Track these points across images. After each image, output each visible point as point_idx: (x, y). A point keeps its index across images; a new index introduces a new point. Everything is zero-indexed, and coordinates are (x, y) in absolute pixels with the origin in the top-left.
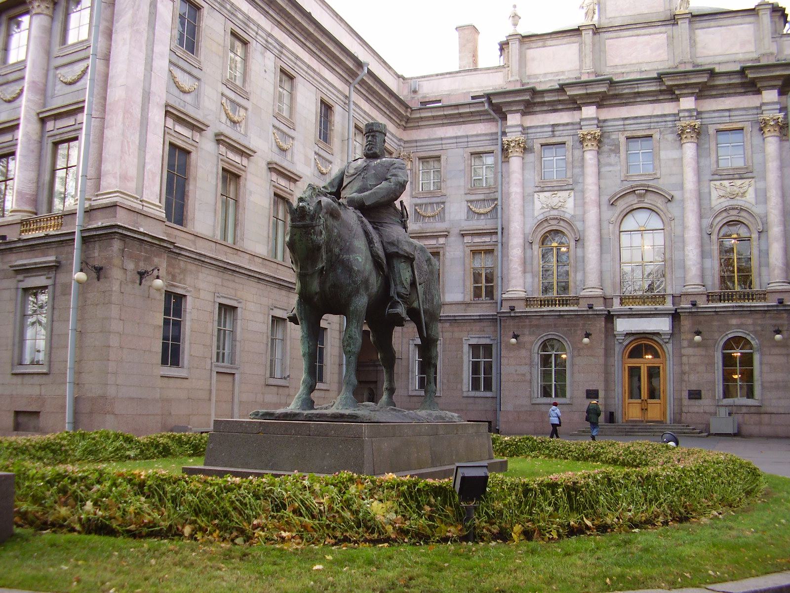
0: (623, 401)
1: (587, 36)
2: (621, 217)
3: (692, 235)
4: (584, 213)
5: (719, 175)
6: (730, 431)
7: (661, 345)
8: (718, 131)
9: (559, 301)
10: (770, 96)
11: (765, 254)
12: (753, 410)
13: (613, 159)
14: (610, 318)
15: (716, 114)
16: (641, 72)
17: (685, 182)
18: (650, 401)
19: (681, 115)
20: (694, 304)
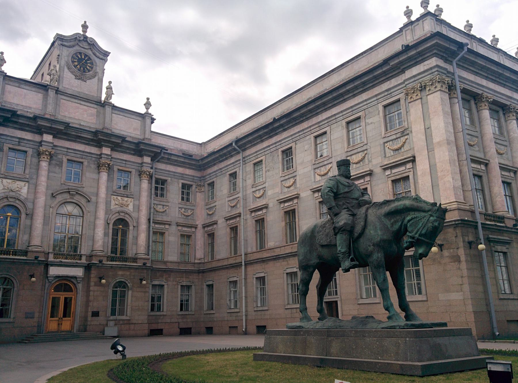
0: (47, 320)
1: (51, 93)
2: (58, 205)
3: (100, 223)
4: (35, 198)
5: (115, 193)
6: (116, 335)
7: (75, 284)
8: (118, 170)
9: (12, 252)
10: (147, 159)
11: (136, 238)
12: (126, 322)
13: (57, 169)
14: (47, 265)
15: (119, 161)
16: (80, 125)
17: (100, 192)
18: (64, 319)
19: (103, 156)
20: (101, 261)
